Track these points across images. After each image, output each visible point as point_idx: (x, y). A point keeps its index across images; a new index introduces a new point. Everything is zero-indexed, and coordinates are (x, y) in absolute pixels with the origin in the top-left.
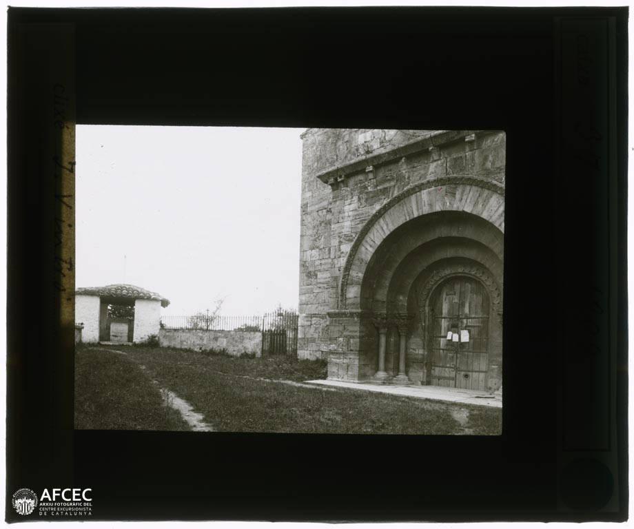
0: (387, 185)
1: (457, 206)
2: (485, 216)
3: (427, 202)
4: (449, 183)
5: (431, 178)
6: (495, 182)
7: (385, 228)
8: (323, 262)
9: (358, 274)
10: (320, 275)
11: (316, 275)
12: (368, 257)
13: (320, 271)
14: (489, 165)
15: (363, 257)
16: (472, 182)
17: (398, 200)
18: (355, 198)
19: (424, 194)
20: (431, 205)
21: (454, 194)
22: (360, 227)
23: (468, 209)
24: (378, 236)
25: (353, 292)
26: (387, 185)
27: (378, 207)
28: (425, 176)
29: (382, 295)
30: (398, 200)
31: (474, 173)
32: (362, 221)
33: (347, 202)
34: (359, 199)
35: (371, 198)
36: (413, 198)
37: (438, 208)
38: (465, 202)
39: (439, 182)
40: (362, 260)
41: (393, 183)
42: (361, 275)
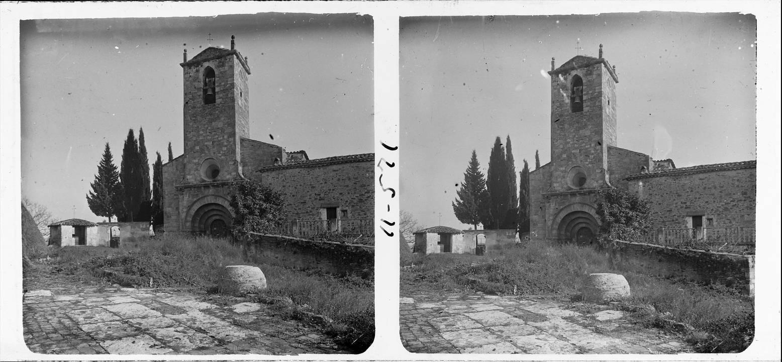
1: (217, 202)
2: (225, 206)
4: (216, 196)
5: (210, 193)
9: (190, 219)
12: (193, 214)
14: (225, 193)
16: (221, 197)
18: (188, 195)
19: (209, 198)
20: (211, 201)
21: (216, 199)
23: (220, 203)
24: (196, 207)
25: (188, 224)
27: (195, 199)
28: (209, 192)
29: (197, 225)
31: (221, 194)
32: (190, 203)
34: (189, 196)
35: (193, 196)
36: (206, 198)
37: (213, 202)
38: (220, 201)
39: (213, 195)
42: (191, 219)
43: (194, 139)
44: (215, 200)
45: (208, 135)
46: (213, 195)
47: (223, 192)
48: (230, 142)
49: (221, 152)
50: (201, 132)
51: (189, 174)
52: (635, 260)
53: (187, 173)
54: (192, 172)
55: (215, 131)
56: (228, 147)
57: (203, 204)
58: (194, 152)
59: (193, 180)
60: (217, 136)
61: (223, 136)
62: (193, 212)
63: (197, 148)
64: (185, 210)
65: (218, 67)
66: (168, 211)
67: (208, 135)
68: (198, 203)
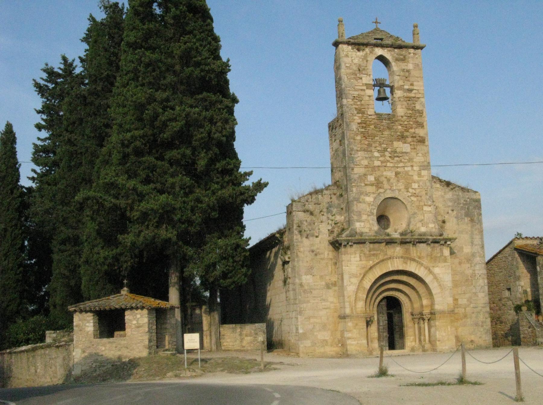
0: (375, 252)
3: (398, 265)
4: (407, 258)
6: (423, 262)
7: (376, 273)
8: (316, 284)
10: (314, 292)
11: (311, 292)
13: (315, 290)
15: (365, 286)
16: (414, 260)
17: (383, 261)
18: (358, 255)
21: (406, 263)
22: (363, 271)
26: (375, 252)
27: (371, 263)
28: (394, 252)
30: (383, 261)
33: (352, 256)
34: (360, 256)
35: (368, 257)
36: (389, 262)
37: (401, 268)
40: (365, 288)
41: (379, 252)
43: (365, 162)
44: (404, 265)
45: (388, 161)
46: (402, 257)
47: (417, 253)
48: (423, 176)
49: (410, 190)
50: (376, 154)
51: (359, 221)
52: (292, 341)
53: (355, 218)
54: (364, 217)
55: (398, 157)
56: (421, 183)
57: (385, 271)
58: (366, 185)
59: (367, 230)
60: (401, 165)
61: (412, 166)
62: (367, 284)
63: (371, 178)
64: (355, 281)
65: (397, 60)
66: (304, 281)
67: (388, 161)
68: (378, 265)
